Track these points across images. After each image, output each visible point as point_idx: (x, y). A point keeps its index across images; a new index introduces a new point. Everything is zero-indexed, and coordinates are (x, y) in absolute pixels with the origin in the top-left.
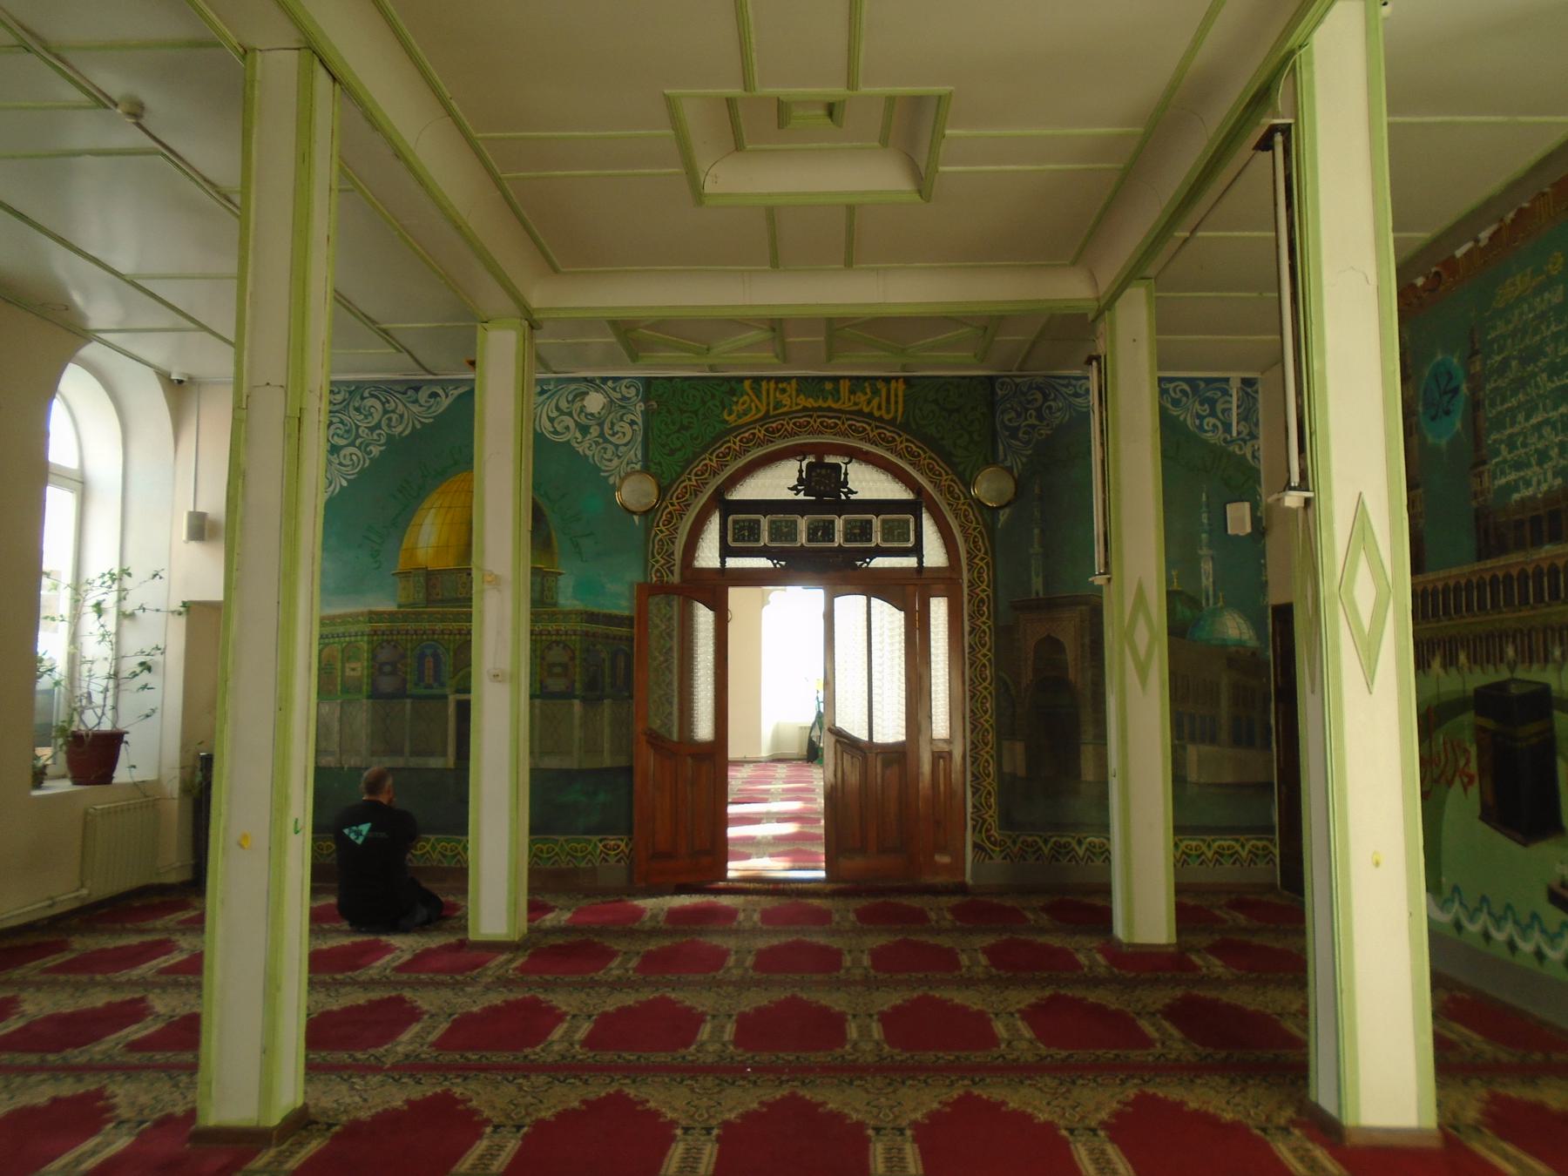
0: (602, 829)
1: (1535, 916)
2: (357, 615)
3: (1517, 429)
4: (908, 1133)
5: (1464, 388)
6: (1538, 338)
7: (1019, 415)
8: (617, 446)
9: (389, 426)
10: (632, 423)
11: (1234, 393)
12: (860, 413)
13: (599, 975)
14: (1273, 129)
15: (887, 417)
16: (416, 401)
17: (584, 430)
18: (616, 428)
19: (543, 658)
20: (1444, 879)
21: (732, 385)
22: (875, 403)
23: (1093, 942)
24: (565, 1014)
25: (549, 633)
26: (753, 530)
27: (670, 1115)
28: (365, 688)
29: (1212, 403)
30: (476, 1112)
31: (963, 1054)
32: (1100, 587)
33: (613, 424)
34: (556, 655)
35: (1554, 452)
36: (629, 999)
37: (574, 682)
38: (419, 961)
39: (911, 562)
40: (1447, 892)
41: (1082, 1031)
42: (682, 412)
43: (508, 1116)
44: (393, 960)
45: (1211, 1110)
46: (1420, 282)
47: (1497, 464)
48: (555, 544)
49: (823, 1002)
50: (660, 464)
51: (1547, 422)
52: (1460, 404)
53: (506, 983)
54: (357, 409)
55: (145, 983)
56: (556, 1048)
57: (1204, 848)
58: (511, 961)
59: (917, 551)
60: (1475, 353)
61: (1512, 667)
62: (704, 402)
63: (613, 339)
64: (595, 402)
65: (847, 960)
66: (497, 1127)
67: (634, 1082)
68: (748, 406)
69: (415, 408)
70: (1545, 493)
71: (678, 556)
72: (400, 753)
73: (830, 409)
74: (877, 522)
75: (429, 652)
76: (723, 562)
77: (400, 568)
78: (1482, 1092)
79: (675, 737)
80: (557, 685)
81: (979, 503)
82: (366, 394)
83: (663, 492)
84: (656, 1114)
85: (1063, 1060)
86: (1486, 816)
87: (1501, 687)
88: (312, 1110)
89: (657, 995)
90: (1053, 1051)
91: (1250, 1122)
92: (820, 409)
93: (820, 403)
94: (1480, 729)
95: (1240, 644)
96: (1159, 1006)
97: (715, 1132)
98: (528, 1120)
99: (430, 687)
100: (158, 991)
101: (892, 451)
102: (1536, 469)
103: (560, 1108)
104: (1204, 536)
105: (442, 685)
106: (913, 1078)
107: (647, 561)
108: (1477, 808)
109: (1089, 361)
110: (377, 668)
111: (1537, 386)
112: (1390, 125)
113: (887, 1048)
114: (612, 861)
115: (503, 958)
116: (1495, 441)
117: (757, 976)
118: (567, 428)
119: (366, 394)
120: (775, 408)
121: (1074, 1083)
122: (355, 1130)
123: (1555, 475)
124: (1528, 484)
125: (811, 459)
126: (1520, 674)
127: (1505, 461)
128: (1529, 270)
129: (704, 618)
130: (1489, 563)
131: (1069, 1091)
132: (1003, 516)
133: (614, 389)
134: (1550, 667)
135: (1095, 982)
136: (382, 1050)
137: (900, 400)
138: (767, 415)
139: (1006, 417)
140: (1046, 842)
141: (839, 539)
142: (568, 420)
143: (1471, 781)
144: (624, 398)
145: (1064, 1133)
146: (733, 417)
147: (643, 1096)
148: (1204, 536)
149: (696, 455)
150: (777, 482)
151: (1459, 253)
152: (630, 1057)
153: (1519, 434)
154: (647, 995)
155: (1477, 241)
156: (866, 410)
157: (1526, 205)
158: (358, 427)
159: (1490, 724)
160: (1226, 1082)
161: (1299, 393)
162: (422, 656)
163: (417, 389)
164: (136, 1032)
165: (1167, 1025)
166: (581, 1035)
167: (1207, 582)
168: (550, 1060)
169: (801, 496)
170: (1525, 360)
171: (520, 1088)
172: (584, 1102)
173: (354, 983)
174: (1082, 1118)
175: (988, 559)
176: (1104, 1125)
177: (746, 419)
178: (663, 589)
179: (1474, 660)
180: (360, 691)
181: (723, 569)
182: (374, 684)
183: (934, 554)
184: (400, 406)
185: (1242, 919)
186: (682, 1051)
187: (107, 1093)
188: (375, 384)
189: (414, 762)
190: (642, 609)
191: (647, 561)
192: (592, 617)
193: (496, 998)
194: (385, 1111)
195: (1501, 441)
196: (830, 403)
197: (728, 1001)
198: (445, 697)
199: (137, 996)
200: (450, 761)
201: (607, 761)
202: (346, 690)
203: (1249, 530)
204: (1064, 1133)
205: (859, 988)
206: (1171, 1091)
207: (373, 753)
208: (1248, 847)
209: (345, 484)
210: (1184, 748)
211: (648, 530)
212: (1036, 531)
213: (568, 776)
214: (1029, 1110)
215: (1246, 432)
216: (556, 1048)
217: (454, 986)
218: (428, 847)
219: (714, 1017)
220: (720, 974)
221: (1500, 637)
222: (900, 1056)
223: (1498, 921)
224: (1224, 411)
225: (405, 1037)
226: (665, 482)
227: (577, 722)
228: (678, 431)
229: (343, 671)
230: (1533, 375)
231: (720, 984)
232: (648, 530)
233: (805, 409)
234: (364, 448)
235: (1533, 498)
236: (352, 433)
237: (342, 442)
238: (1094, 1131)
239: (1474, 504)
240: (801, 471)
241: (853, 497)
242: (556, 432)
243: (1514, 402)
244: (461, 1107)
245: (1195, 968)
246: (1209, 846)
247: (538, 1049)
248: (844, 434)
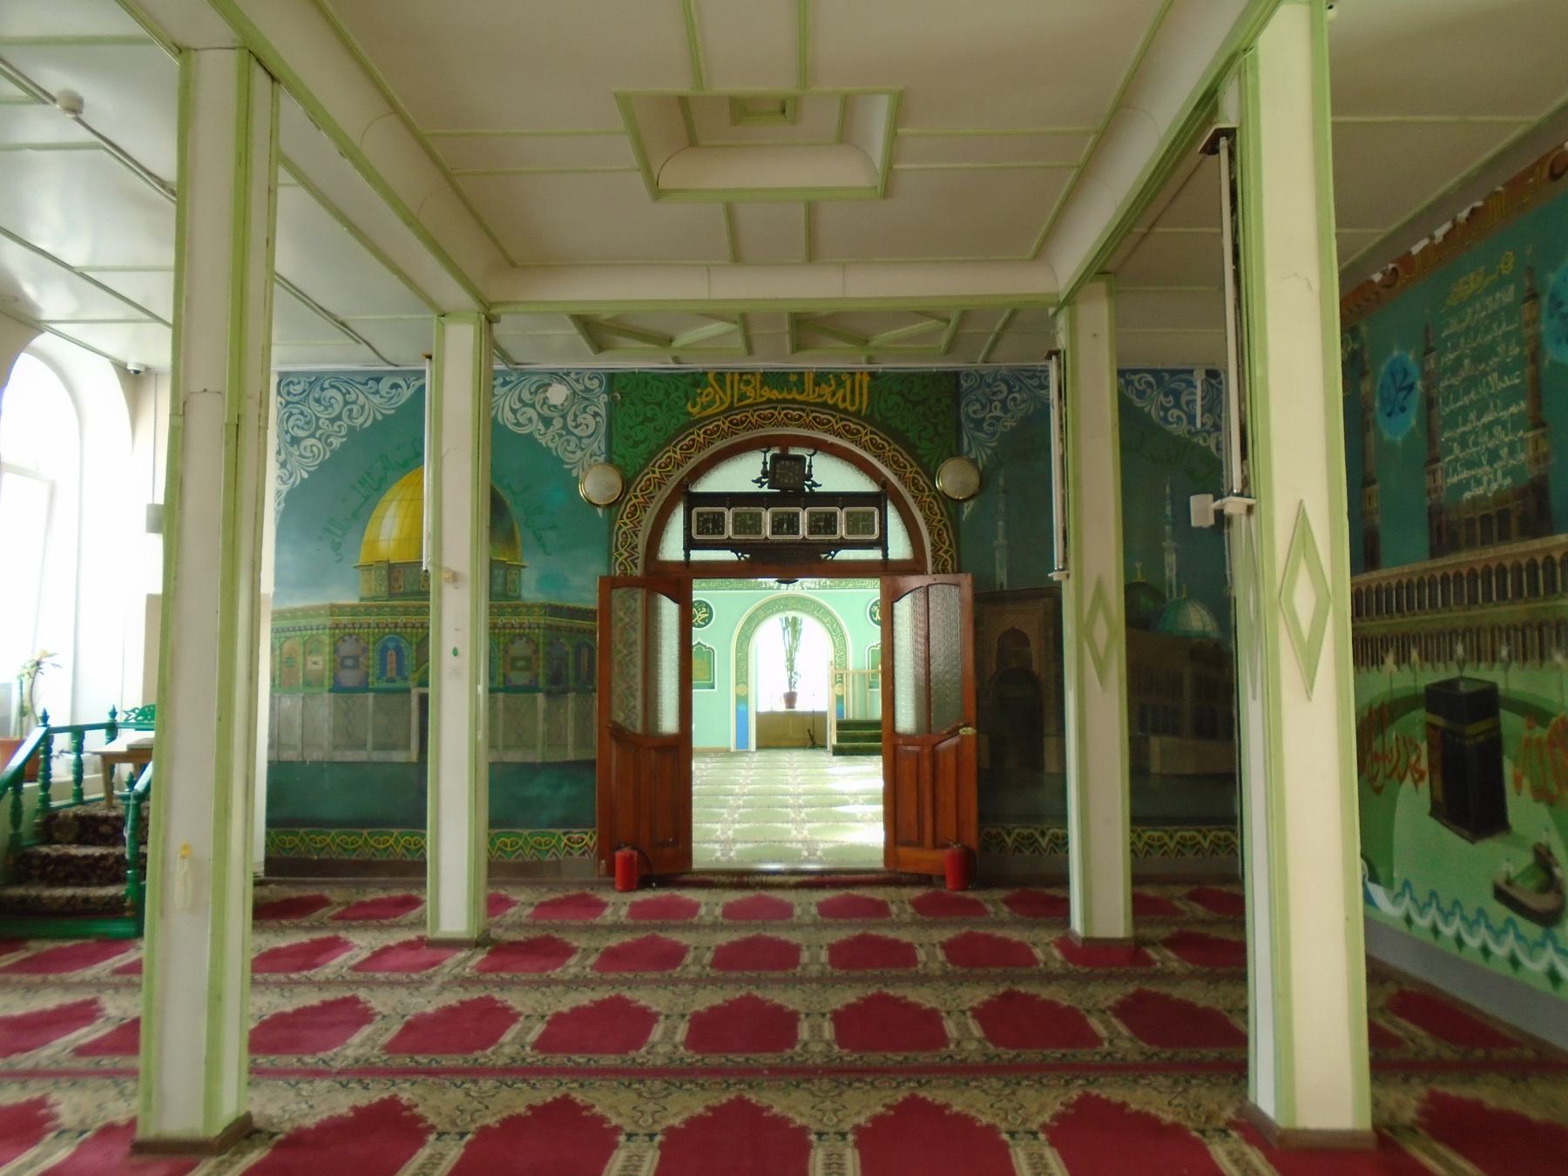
0: (568, 823)
1: (1481, 912)
2: (318, 608)
3: (1468, 428)
4: (850, 1137)
5: (1419, 385)
7: (983, 407)
8: (580, 438)
9: (350, 417)
10: (596, 415)
11: (1199, 384)
12: (824, 405)
13: (557, 973)
14: (1220, 133)
15: (851, 409)
16: (377, 392)
17: (547, 422)
18: (579, 420)
19: (506, 651)
21: (697, 380)
22: (840, 394)
23: (1056, 935)
24: (519, 1014)
25: (513, 627)
26: (717, 523)
27: (615, 1121)
28: (326, 682)
29: (1177, 394)
30: (421, 1119)
31: (912, 1055)
32: (1060, 583)
33: (576, 416)
34: (520, 648)
35: (1504, 452)
36: (584, 998)
37: (537, 676)
38: (378, 958)
39: (875, 555)
40: (1398, 887)
41: (1029, 1030)
42: (646, 403)
43: (454, 1123)
44: (351, 958)
45: (1153, 1111)
46: (1377, 277)
48: (518, 536)
49: (777, 1001)
50: (623, 457)
51: (1497, 421)
52: (1415, 401)
53: (464, 982)
54: (318, 401)
55: (98, 984)
56: (507, 1050)
57: (1167, 839)
58: (468, 959)
59: (882, 543)
60: (1429, 351)
61: (1461, 665)
62: (667, 394)
63: (574, 331)
64: (558, 394)
65: (805, 957)
66: (440, 1135)
67: (582, 1085)
68: (714, 399)
69: (376, 399)
70: (1495, 493)
71: (641, 549)
72: (363, 746)
73: (794, 401)
74: (841, 515)
75: (391, 645)
76: (687, 555)
77: (361, 561)
78: (1422, 1091)
79: (639, 729)
80: (519, 678)
81: (943, 497)
82: (326, 385)
83: (627, 485)
84: (601, 1120)
85: (1010, 1060)
86: (1436, 811)
87: (1451, 684)
88: (255, 1119)
89: (613, 994)
90: (1001, 1050)
91: (1190, 1124)
92: (785, 401)
93: (785, 395)
94: (1431, 727)
95: (1204, 635)
96: (1110, 1003)
97: (658, 1138)
98: (473, 1127)
99: (392, 681)
100: (110, 992)
101: (856, 443)
102: (1487, 468)
103: (505, 1114)
104: (1167, 528)
105: (405, 679)
106: (859, 1080)
107: (610, 555)
108: (1428, 806)
109: (1049, 357)
110: (339, 663)
112: (1334, 124)
113: (836, 1048)
114: (576, 854)
115: (461, 955)
116: (1448, 439)
117: (713, 973)
118: (530, 420)
119: (326, 385)
120: (739, 400)
121: (1019, 1084)
122: (297, 1141)
123: (1504, 476)
124: (1479, 482)
125: (776, 451)
126: (1469, 672)
127: (1457, 459)
128: (1482, 269)
129: (669, 611)
130: (1440, 562)
131: (1014, 1093)
132: (967, 508)
133: (577, 381)
134: (1498, 665)
135: (1049, 978)
136: (330, 1053)
137: (865, 391)
138: (731, 408)
139: (971, 409)
140: (1009, 834)
141: (803, 531)
142: (531, 412)
143: (1422, 777)
144: (587, 390)
145: (1005, 1137)
146: (697, 409)
147: (589, 1101)
148: (1167, 528)
149: (660, 447)
150: (741, 475)
151: (1416, 249)
152: (581, 1059)
153: (1470, 432)
154: (602, 994)
155: (1432, 238)
156: (831, 402)
157: (1478, 204)
158: (318, 419)
159: (1439, 721)
160: (1169, 1082)
161: (1241, 399)
162: (384, 650)
163: (378, 380)
164: (84, 1035)
165: (1115, 1021)
166: (532, 1037)
167: (1170, 573)
168: (500, 1063)
169: (765, 489)
171: (468, 1094)
172: (530, 1107)
173: (309, 982)
174: (1025, 1121)
175: (952, 551)
176: (1044, 1127)
177: (710, 411)
178: (628, 582)
179: (1426, 657)
180: (321, 685)
181: (687, 563)
182: (335, 677)
183: (899, 547)
184: (362, 398)
185: (1200, 911)
186: (632, 1053)
187: (51, 1100)
188: (335, 375)
189: (377, 756)
190: (605, 601)
191: (610, 555)
192: (554, 610)
193: (452, 998)
194: (331, 1117)
195: (1453, 440)
196: (795, 395)
197: (682, 1000)
198: (408, 691)
199: (89, 997)
200: (414, 756)
201: (571, 755)
202: (307, 684)
203: (1211, 521)
204: (1005, 1137)
205: (815, 986)
206: (1113, 1092)
207: (336, 747)
208: (1211, 836)
209: (305, 475)
210: (1147, 739)
211: (612, 523)
212: (1001, 523)
213: (531, 769)
214: (973, 1113)
215: (1210, 423)
216: (507, 1050)
217: (407, 985)
218: (391, 841)
219: (667, 1017)
220: (677, 972)
221: (1450, 634)
222: (850, 1057)
223: (1447, 916)
224: (1188, 403)
225: (356, 1039)
226: (630, 475)
227: (541, 715)
228: (642, 423)
229: (305, 665)
230: (1485, 374)
231: (675, 982)
232: (612, 523)
233: (769, 401)
234: (325, 439)
235: (1484, 497)
236: (312, 425)
237: (301, 433)
238: (1034, 1134)
239: (1428, 502)
240: (765, 463)
241: (816, 489)
242: (518, 424)
243: (1466, 400)
244: (405, 1113)
245: (1150, 962)
246: (1171, 837)
247: (489, 1051)
248: (809, 426)
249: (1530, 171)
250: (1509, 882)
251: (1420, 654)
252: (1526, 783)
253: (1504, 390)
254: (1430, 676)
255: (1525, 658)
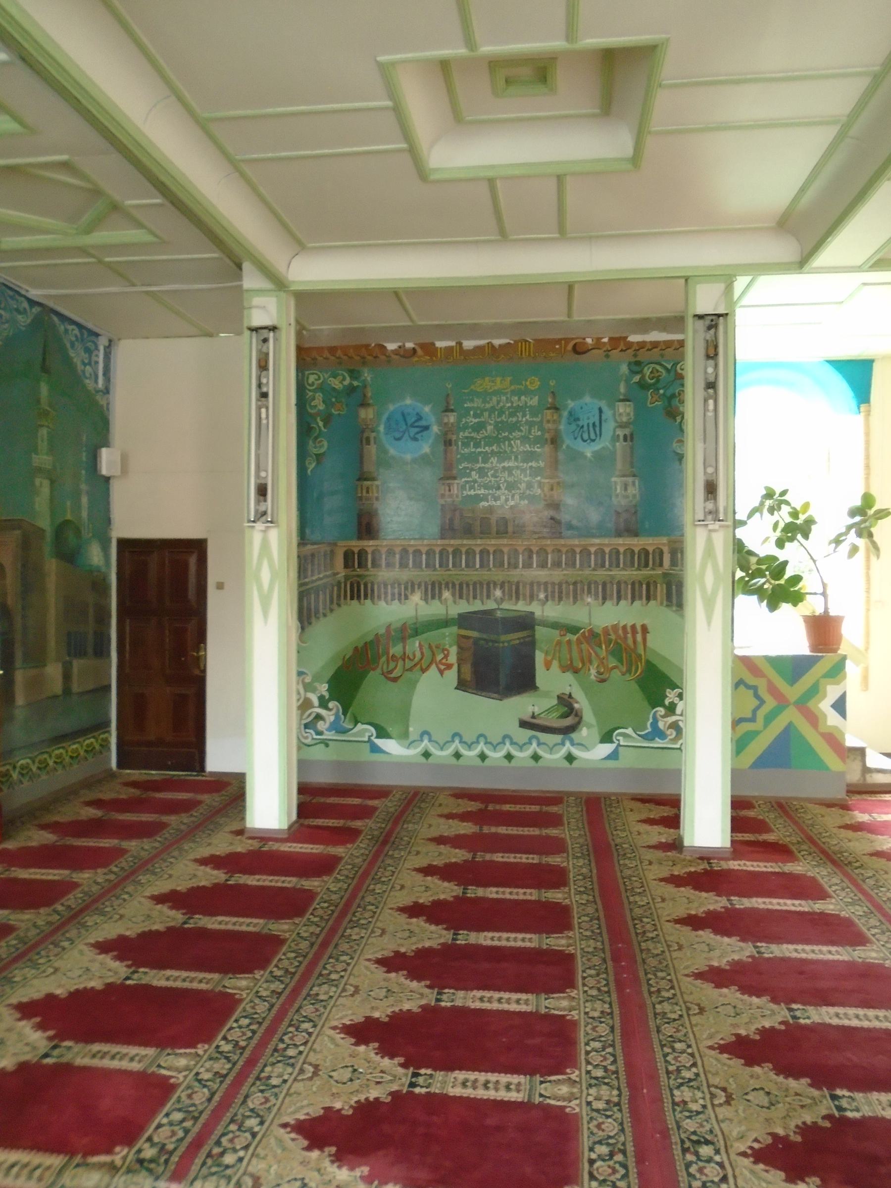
5: (435, 429)
6: (514, 419)
20: (411, 729)
46: (391, 346)
47: (467, 482)
60: (447, 410)
102: (503, 491)
104: (83, 472)
111: (510, 445)
116: (464, 468)
123: (521, 498)
126: (505, 606)
128: (509, 379)
134: (535, 603)
143: (449, 667)
167: (84, 514)
170: (499, 427)
210: (71, 663)
221: (488, 584)
239: (442, 502)
249: (558, 341)
250: (533, 717)
251: (453, 595)
252: (555, 664)
253: (524, 452)
254: (464, 607)
255: (560, 599)
